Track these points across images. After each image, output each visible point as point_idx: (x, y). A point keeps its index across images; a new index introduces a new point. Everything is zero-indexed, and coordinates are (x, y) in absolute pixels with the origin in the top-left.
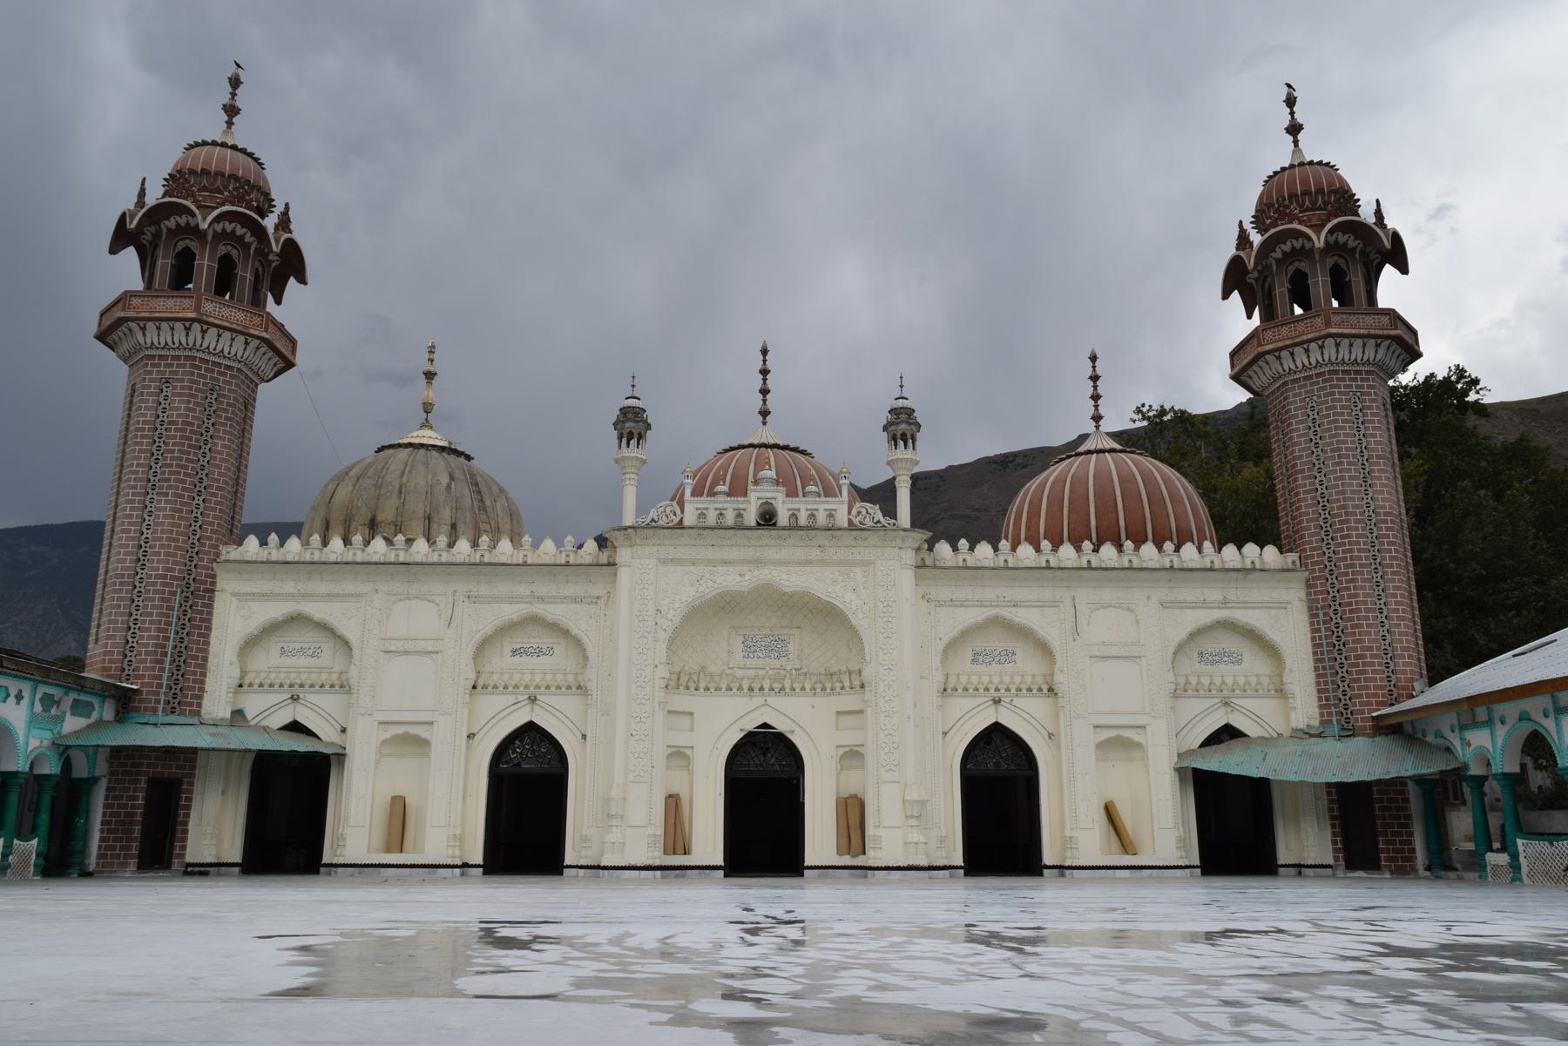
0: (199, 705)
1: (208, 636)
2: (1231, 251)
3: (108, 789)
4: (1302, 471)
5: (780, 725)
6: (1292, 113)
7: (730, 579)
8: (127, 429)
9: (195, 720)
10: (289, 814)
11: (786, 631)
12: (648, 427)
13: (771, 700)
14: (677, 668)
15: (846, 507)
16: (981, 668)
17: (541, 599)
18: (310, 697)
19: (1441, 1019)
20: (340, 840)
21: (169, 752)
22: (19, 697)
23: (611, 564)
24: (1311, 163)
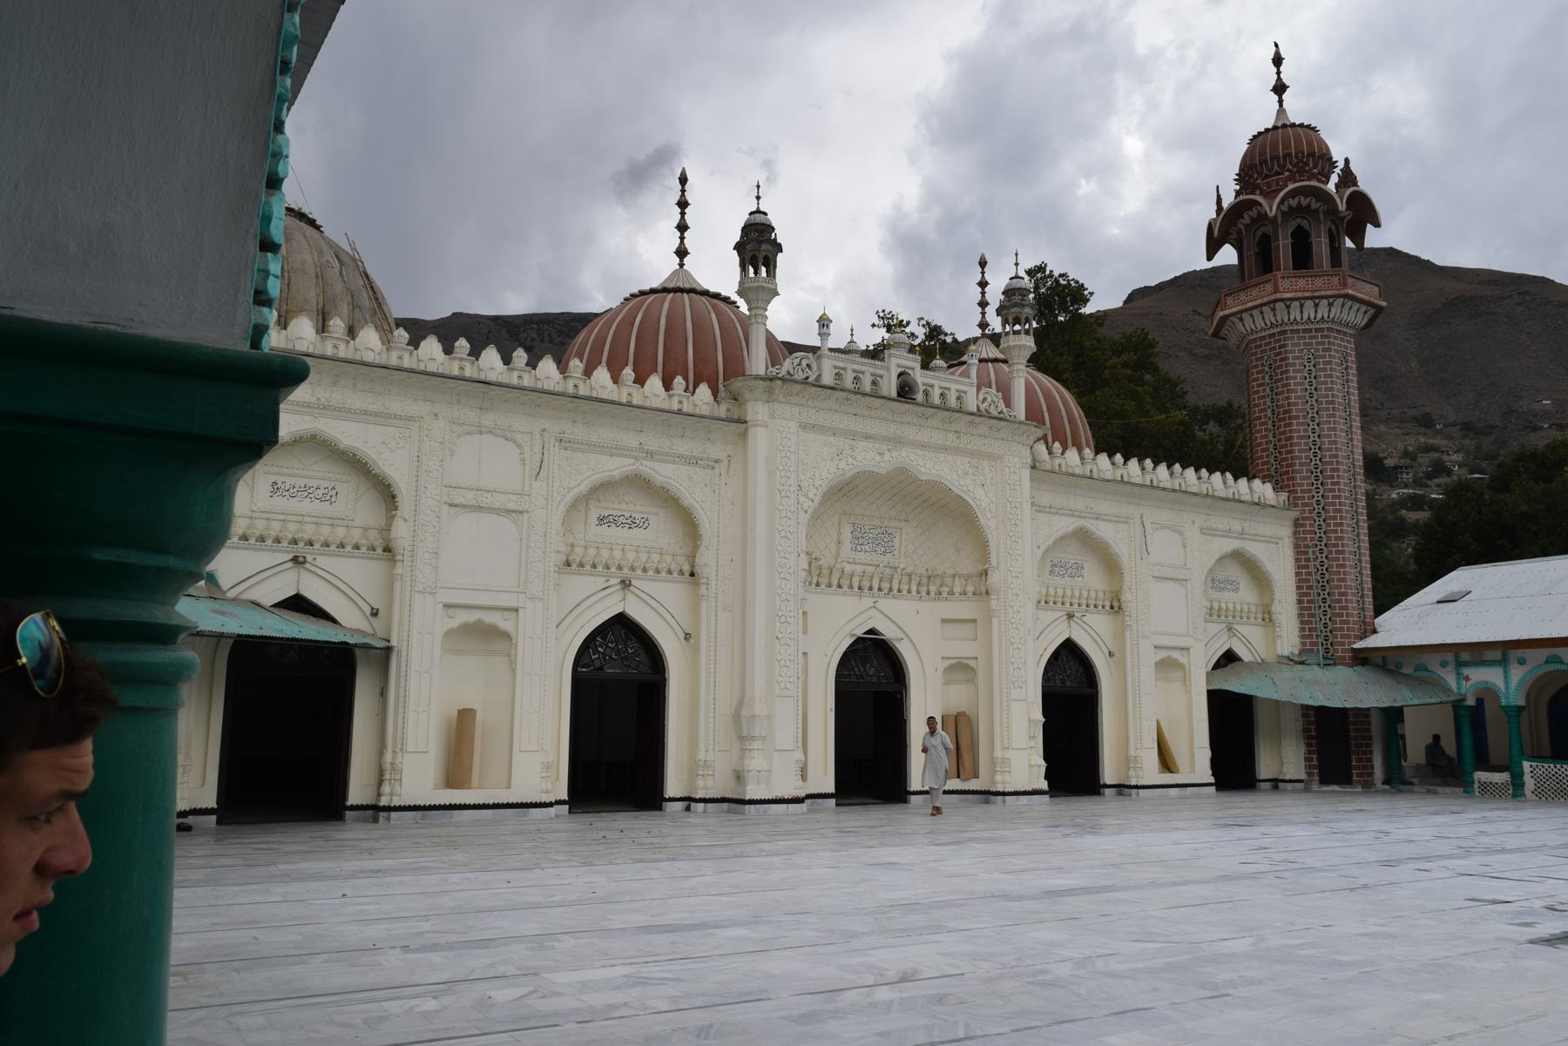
4: (1297, 417)
5: (888, 632)
7: (870, 458)
11: (896, 524)
16: (1057, 580)
17: (651, 455)
18: (322, 561)
19: (1529, 920)
24: (1293, 125)
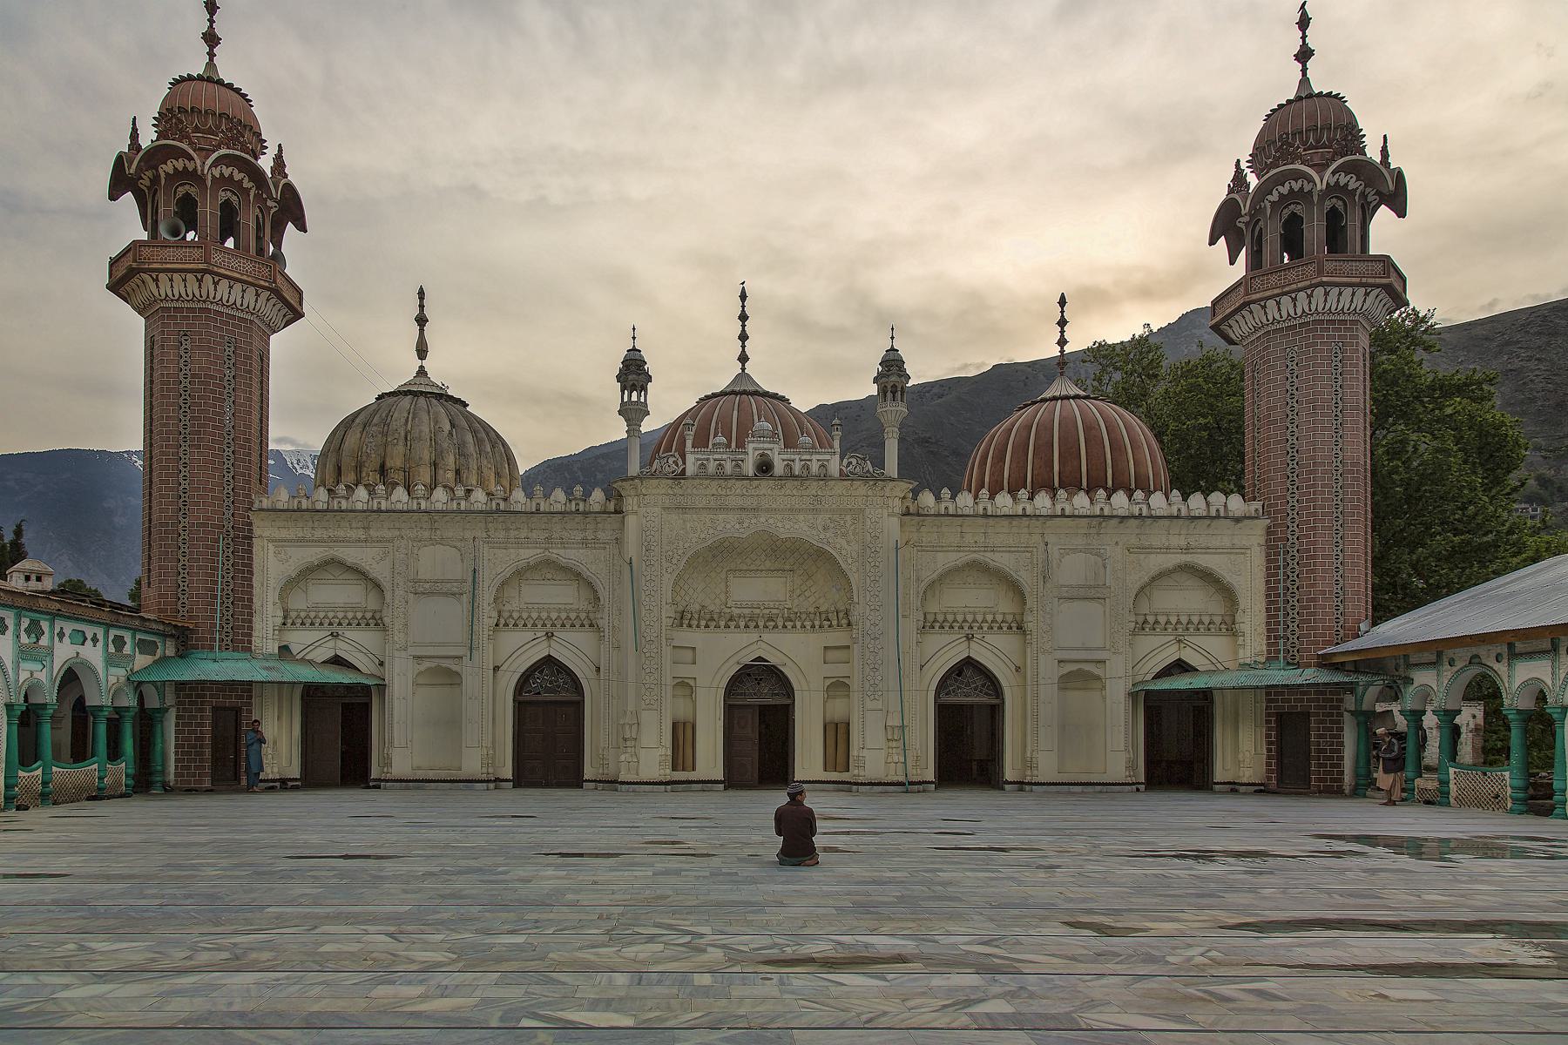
0: (250, 642)
1: (251, 580)
2: (1222, 195)
3: (177, 717)
5: (773, 659)
6: (1304, 37)
8: (152, 382)
9: (248, 655)
10: (343, 732)
12: (649, 379)
13: (765, 637)
14: (681, 608)
18: (348, 634)
20: (387, 762)
21: (232, 685)
22: (95, 640)
23: (618, 511)
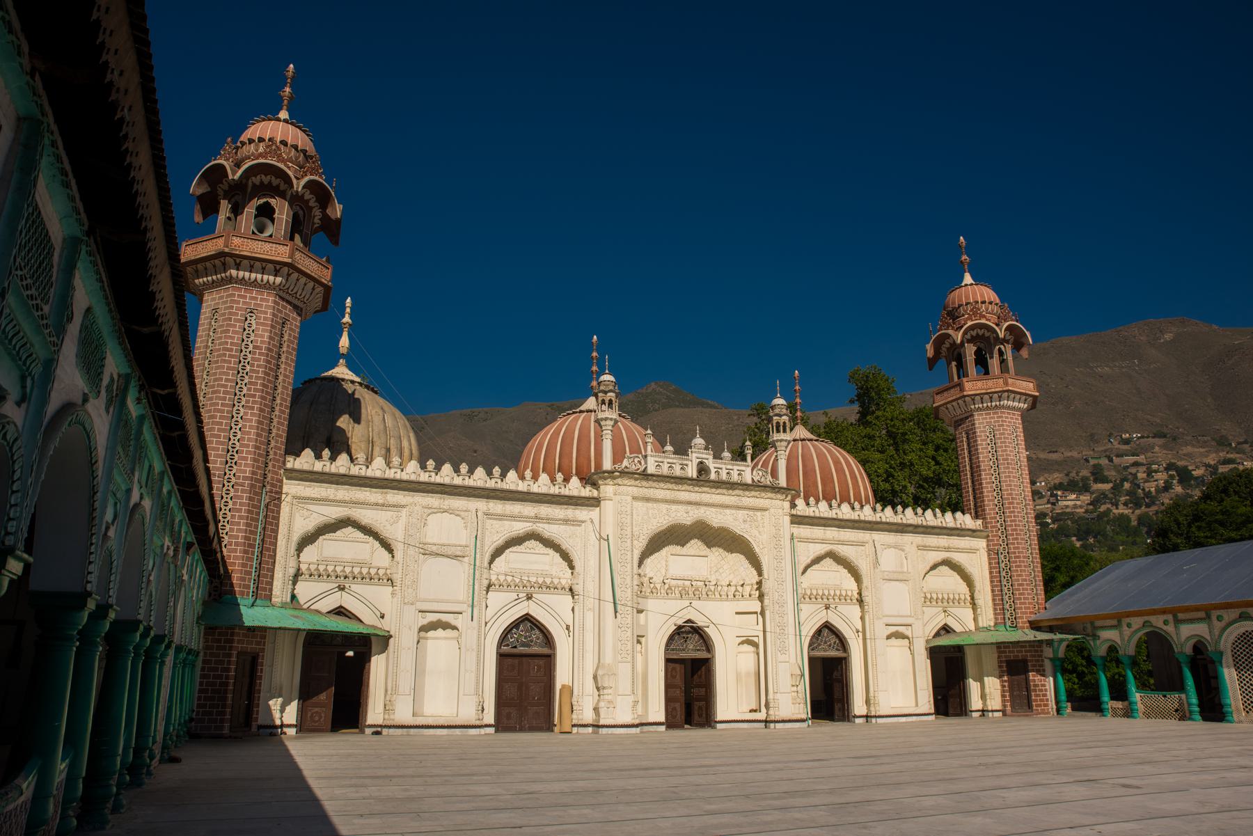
15: (749, 469)
